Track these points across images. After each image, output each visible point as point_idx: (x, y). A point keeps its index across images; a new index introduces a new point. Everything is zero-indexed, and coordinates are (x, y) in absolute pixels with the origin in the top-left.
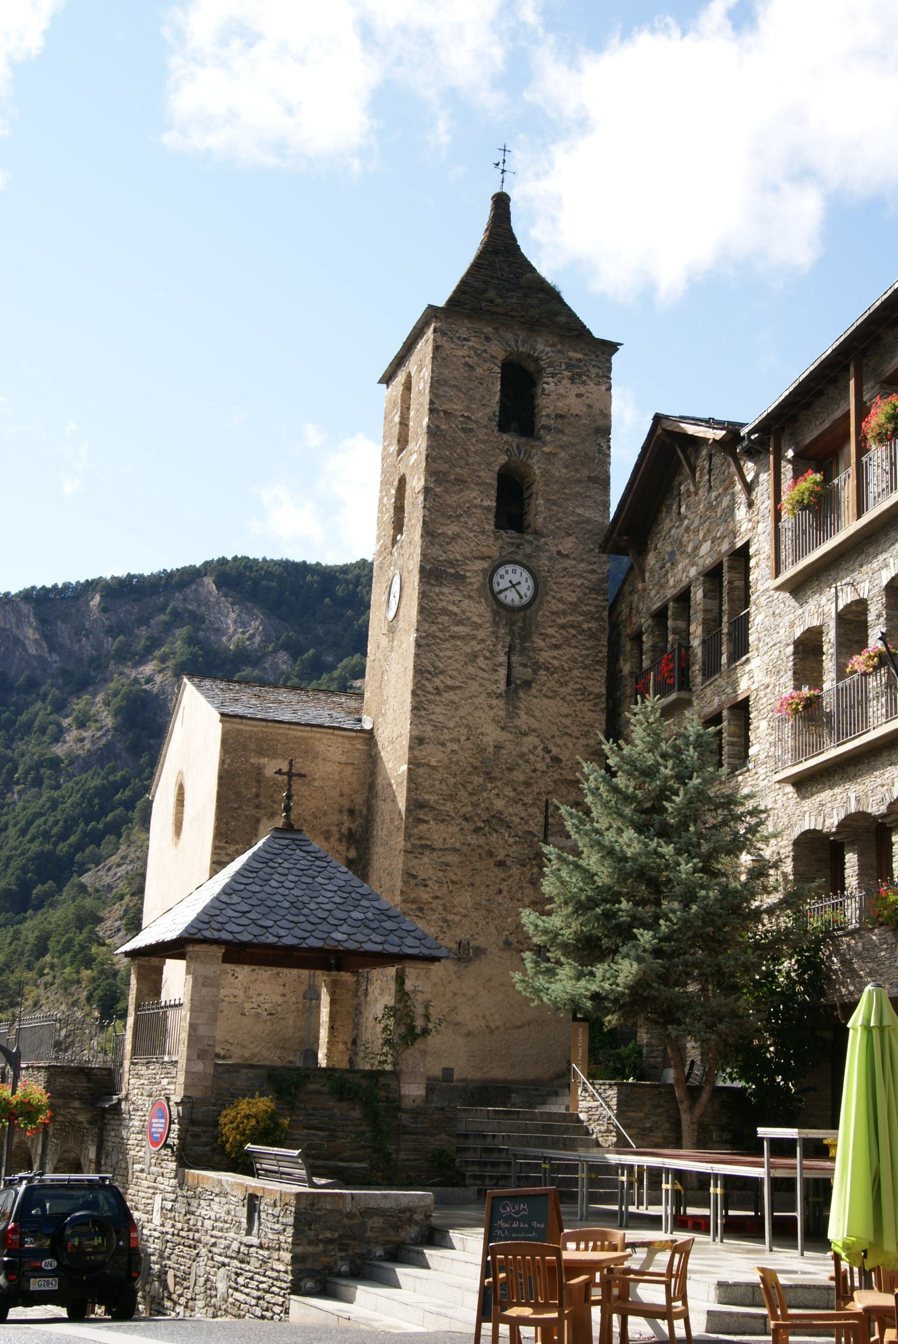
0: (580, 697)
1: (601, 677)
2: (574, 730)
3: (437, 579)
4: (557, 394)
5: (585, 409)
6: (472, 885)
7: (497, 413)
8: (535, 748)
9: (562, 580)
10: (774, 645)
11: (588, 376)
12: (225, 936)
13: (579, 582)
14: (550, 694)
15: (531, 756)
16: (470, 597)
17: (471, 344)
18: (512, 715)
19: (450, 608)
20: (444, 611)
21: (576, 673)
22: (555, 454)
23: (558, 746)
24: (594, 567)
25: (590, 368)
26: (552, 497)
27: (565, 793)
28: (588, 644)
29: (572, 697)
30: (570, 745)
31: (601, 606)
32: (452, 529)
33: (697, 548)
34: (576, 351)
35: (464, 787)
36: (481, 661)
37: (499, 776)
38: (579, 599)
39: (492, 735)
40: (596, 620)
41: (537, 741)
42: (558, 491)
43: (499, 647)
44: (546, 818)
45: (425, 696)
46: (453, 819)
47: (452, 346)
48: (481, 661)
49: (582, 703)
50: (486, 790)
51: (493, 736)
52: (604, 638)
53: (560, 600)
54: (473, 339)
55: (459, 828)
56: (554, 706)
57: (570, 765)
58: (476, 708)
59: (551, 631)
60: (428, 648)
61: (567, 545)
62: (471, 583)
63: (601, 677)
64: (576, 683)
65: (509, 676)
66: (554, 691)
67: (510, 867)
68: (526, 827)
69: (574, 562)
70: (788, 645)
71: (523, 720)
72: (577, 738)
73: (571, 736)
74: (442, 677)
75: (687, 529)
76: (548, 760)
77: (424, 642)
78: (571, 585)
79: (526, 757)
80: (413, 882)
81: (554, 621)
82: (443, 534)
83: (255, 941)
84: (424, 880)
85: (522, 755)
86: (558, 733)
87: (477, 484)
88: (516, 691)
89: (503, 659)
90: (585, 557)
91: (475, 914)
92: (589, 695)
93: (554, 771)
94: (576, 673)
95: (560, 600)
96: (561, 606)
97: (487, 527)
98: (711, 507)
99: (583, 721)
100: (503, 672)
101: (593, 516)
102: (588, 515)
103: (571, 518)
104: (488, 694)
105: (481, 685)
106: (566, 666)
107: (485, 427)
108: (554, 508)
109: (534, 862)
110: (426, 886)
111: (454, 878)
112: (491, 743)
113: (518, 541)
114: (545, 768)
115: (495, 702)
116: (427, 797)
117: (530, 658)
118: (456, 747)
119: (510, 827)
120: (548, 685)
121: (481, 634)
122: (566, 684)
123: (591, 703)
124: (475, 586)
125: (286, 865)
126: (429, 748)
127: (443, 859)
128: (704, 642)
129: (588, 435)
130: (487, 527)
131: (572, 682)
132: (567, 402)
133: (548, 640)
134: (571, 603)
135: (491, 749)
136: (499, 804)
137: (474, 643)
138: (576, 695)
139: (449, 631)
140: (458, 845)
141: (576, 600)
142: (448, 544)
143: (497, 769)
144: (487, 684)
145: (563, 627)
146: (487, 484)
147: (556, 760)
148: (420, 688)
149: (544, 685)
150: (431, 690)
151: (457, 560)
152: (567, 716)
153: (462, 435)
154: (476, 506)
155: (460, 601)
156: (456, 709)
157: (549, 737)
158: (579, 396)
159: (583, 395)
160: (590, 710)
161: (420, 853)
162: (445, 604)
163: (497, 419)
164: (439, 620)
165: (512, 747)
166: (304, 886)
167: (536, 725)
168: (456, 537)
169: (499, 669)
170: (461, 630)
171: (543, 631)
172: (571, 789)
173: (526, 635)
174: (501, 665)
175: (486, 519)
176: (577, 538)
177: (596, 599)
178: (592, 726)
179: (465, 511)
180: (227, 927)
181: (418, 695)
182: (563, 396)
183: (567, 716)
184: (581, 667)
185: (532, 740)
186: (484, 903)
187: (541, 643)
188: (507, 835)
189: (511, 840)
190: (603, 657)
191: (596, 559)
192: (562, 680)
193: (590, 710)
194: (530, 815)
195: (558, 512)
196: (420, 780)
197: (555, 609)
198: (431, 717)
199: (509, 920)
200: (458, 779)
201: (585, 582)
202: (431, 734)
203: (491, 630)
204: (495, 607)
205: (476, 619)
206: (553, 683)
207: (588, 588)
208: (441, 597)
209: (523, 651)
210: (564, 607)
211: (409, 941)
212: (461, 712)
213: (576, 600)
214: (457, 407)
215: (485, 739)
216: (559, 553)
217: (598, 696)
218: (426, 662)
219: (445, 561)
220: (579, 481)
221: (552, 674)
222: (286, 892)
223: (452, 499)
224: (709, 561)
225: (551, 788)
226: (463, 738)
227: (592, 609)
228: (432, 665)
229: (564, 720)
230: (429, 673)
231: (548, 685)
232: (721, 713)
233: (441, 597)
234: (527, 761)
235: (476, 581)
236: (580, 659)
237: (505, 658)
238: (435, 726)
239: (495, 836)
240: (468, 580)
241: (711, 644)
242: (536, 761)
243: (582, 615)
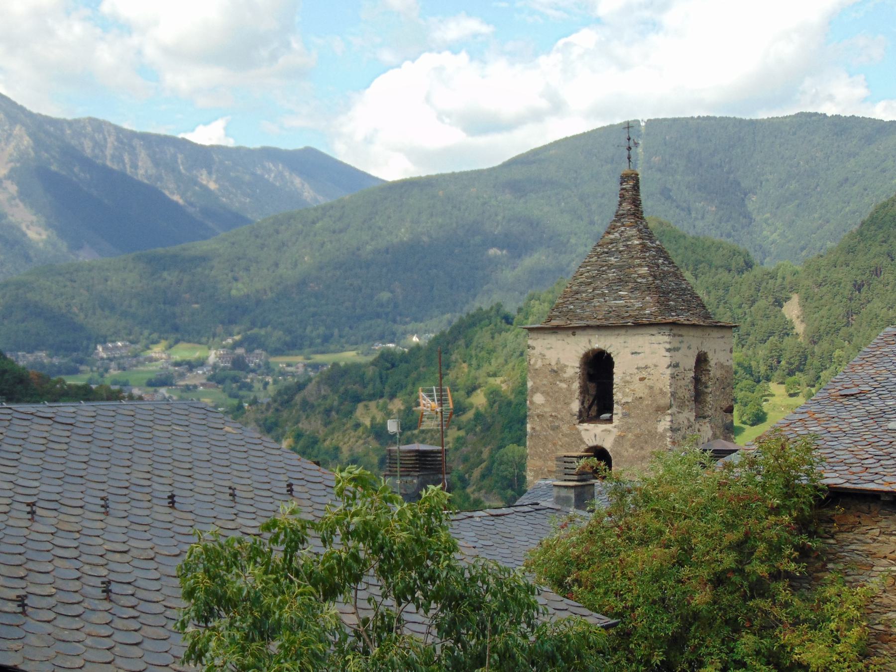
5: (647, 391)
129: (650, 414)
153: (551, 432)
159: (645, 378)
182: (628, 382)
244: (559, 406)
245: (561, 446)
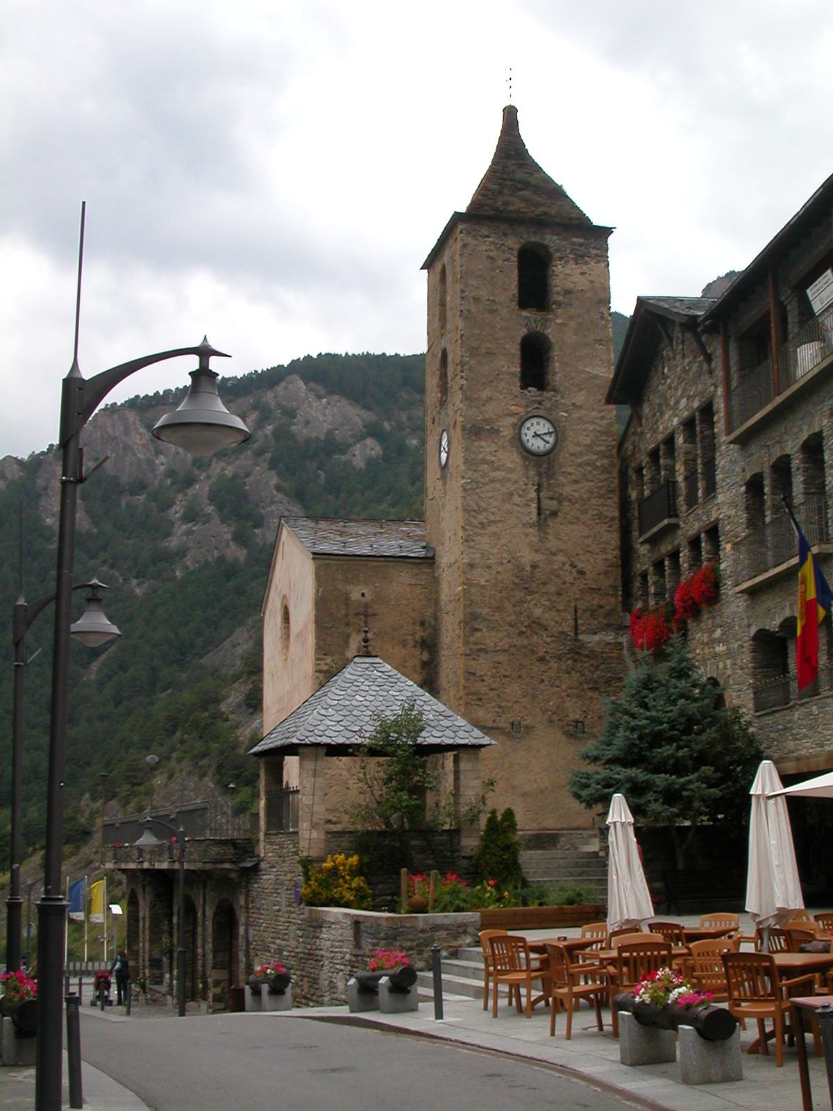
0: (597, 521)
1: (614, 503)
4: (565, 274)
6: (520, 677)
7: (517, 295)
8: (564, 564)
10: (733, 485)
11: (589, 257)
12: (325, 740)
13: (591, 427)
14: (574, 521)
16: (504, 447)
17: (491, 239)
20: (484, 461)
21: (593, 501)
22: (566, 325)
24: (603, 414)
25: (591, 250)
27: (590, 598)
28: (601, 477)
30: (592, 561)
32: (486, 394)
33: (677, 403)
34: (578, 237)
35: (508, 600)
36: (516, 499)
37: (536, 590)
38: (592, 441)
39: (527, 556)
40: (607, 457)
41: (564, 559)
42: (570, 355)
44: (576, 620)
46: (501, 626)
47: (475, 242)
48: (516, 499)
49: (599, 526)
50: (525, 602)
51: (530, 558)
52: (615, 474)
53: (578, 444)
54: (493, 235)
55: (505, 633)
58: (514, 537)
59: (570, 470)
61: (580, 398)
62: (503, 436)
64: (594, 509)
65: (539, 509)
66: (577, 518)
67: (549, 661)
68: (560, 629)
70: (741, 486)
71: (552, 544)
72: (597, 554)
74: (485, 514)
75: (670, 387)
76: (575, 574)
77: (469, 487)
78: (585, 430)
80: (472, 678)
81: (572, 461)
83: (348, 742)
84: (481, 676)
85: (553, 572)
86: (582, 552)
89: (533, 495)
90: (595, 406)
91: (523, 700)
94: (593, 501)
95: (578, 444)
96: (578, 449)
98: (685, 372)
99: (601, 540)
100: (534, 505)
102: (596, 372)
104: (523, 524)
105: (517, 517)
107: (508, 307)
109: (568, 656)
110: (483, 681)
111: (506, 673)
112: (528, 564)
113: (539, 398)
116: (479, 610)
117: (555, 492)
118: (500, 569)
119: (547, 630)
121: (514, 477)
122: (584, 512)
123: (607, 525)
124: (508, 439)
125: (367, 683)
126: (477, 572)
127: (496, 659)
128: (686, 478)
130: (514, 389)
132: (572, 279)
133: (568, 477)
134: (586, 445)
135: (528, 568)
136: (537, 612)
140: (506, 647)
142: (483, 405)
143: (534, 585)
145: (580, 465)
147: (581, 572)
149: (567, 514)
151: (492, 419)
152: (588, 537)
154: (504, 373)
156: (499, 539)
158: (582, 274)
159: (585, 273)
160: (606, 531)
161: (477, 656)
163: (516, 299)
164: (480, 468)
166: (381, 698)
167: (563, 547)
168: (490, 399)
171: (564, 470)
172: (595, 596)
173: (550, 474)
177: (606, 440)
178: (609, 544)
180: (326, 733)
181: (467, 530)
182: (569, 275)
183: (588, 537)
185: (561, 558)
186: (530, 691)
187: (565, 481)
188: (545, 636)
189: (549, 640)
190: (614, 487)
192: (582, 508)
193: (606, 531)
194: (563, 619)
196: (473, 598)
199: (551, 703)
200: (503, 594)
204: (525, 454)
205: (509, 465)
207: (599, 432)
211: (461, 734)
212: (504, 541)
213: (589, 442)
214: (483, 293)
215: (523, 560)
216: (574, 404)
217: (612, 519)
218: (472, 503)
219: (482, 420)
221: (574, 504)
222: (368, 704)
224: (686, 414)
225: (578, 596)
226: (505, 561)
227: (603, 448)
228: (477, 504)
230: (475, 511)
232: (699, 536)
234: (557, 576)
235: (507, 433)
236: (596, 490)
238: (482, 554)
239: (535, 637)
240: (501, 434)
241: (691, 478)
244: (497, 291)
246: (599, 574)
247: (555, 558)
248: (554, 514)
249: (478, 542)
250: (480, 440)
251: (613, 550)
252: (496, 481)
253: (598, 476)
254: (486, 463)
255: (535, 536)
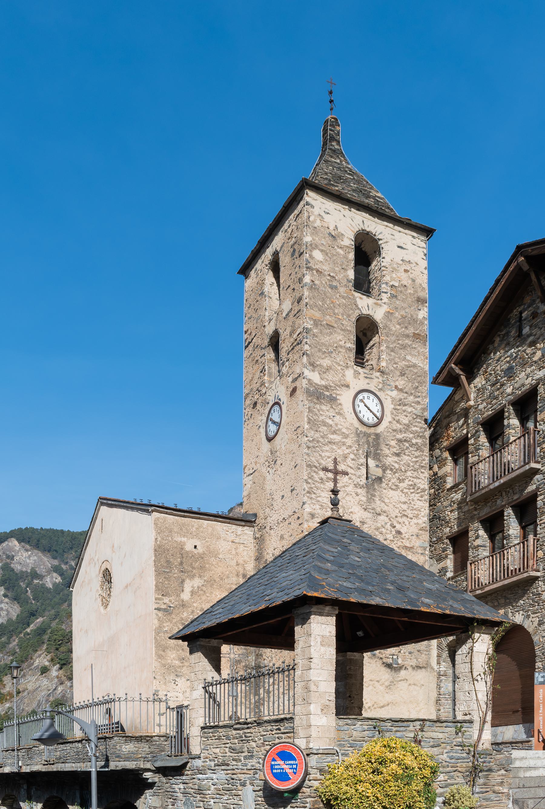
2: (409, 513)
3: (318, 398)
9: (398, 407)
13: (410, 409)
14: (394, 487)
15: (383, 530)
18: (371, 498)
19: (327, 421)
20: (325, 424)
21: (409, 474)
23: (400, 523)
26: (391, 346)
29: (407, 490)
30: (407, 523)
31: (424, 428)
38: (410, 421)
40: (421, 437)
41: (386, 519)
43: (361, 452)
45: (314, 484)
49: (414, 494)
56: (395, 495)
57: (407, 537)
58: (347, 494)
60: (314, 449)
63: (425, 477)
64: (410, 480)
69: (406, 395)
71: (378, 505)
72: (411, 518)
73: (407, 517)
76: (394, 533)
78: (404, 411)
79: (381, 530)
81: (394, 436)
82: (320, 365)
85: (377, 529)
86: (399, 515)
87: (342, 330)
88: (373, 484)
90: (413, 392)
92: (418, 489)
93: (398, 540)
96: (399, 426)
97: (349, 363)
99: (415, 507)
101: (417, 362)
102: (414, 362)
103: (403, 362)
104: (354, 484)
105: (350, 478)
106: (403, 469)
108: (393, 354)
112: (358, 519)
114: (392, 538)
115: (359, 491)
120: (393, 481)
122: (403, 481)
130: (349, 363)
131: (407, 480)
134: (405, 424)
137: (344, 448)
138: (409, 489)
139: (327, 438)
141: (408, 422)
144: (353, 477)
145: (400, 441)
146: (348, 331)
147: (399, 532)
148: (310, 478)
149: (389, 481)
150: (318, 480)
151: (331, 386)
152: (405, 503)
154: (341, 347)
155: (334, 416)
157: (394, 517)
160: (418, 500)
162: (324, 417)
164: (320, 429)
165: (372, 523)
167: (385, 508)
168: (328, 369)
169: (361, 467)
170: (336, 438)
171: (388, 442)
174: (362, 465)
175: (348, 357)
176: (407, 377)
178: (420, 510)
179: (334, 350)
181: (309, 483)
183: (405, 503)
184: (412, 470)
185: (383, 518)
190: (425, 464)
191: (420, 394)
192: (401, 478)
193: (418, 500)
195: (395, 357)
197: (395, 428)
198: (319, 499)
201: (413, 410)
202: (319, 511)
203: (355, 439)
205: (344, 430)
206: (395, 479)
208: (321, 412)
209: (377, 457)
210: (401, 426)
213: (408, 422)
217: (424, 490)
218: (313, 459)
220: (407, 336)
221: (395, 473)
223: (325, 339)
227: (418, 429)
228: (317, 461)
229: (403, 506)
231: (393, 481)
233: (321, 412)
236: (412, 464)
237: (365, 460)
238: (322, 505)
240: (338, 401)
242: (386, 533)
243: (411, 433)
245: (339, 305)
246: (412, 535)
247: (379, 517)
248: (379, 479)
249: (318, 495)
250: (321, 403)
251: (423, 517)
252: (334, 443)
253: (413, 452)
254: (325, 426)
255: (364, 496)
